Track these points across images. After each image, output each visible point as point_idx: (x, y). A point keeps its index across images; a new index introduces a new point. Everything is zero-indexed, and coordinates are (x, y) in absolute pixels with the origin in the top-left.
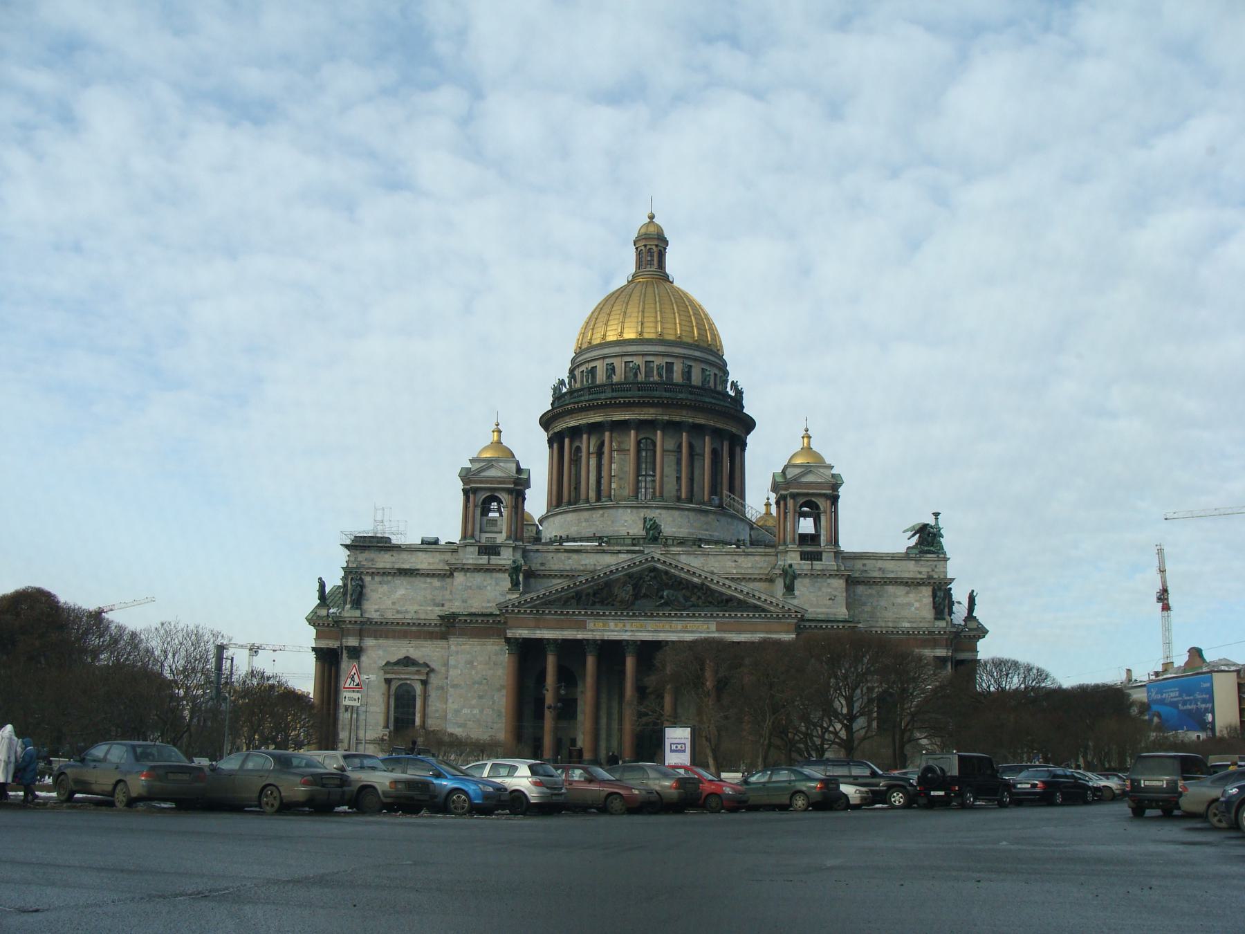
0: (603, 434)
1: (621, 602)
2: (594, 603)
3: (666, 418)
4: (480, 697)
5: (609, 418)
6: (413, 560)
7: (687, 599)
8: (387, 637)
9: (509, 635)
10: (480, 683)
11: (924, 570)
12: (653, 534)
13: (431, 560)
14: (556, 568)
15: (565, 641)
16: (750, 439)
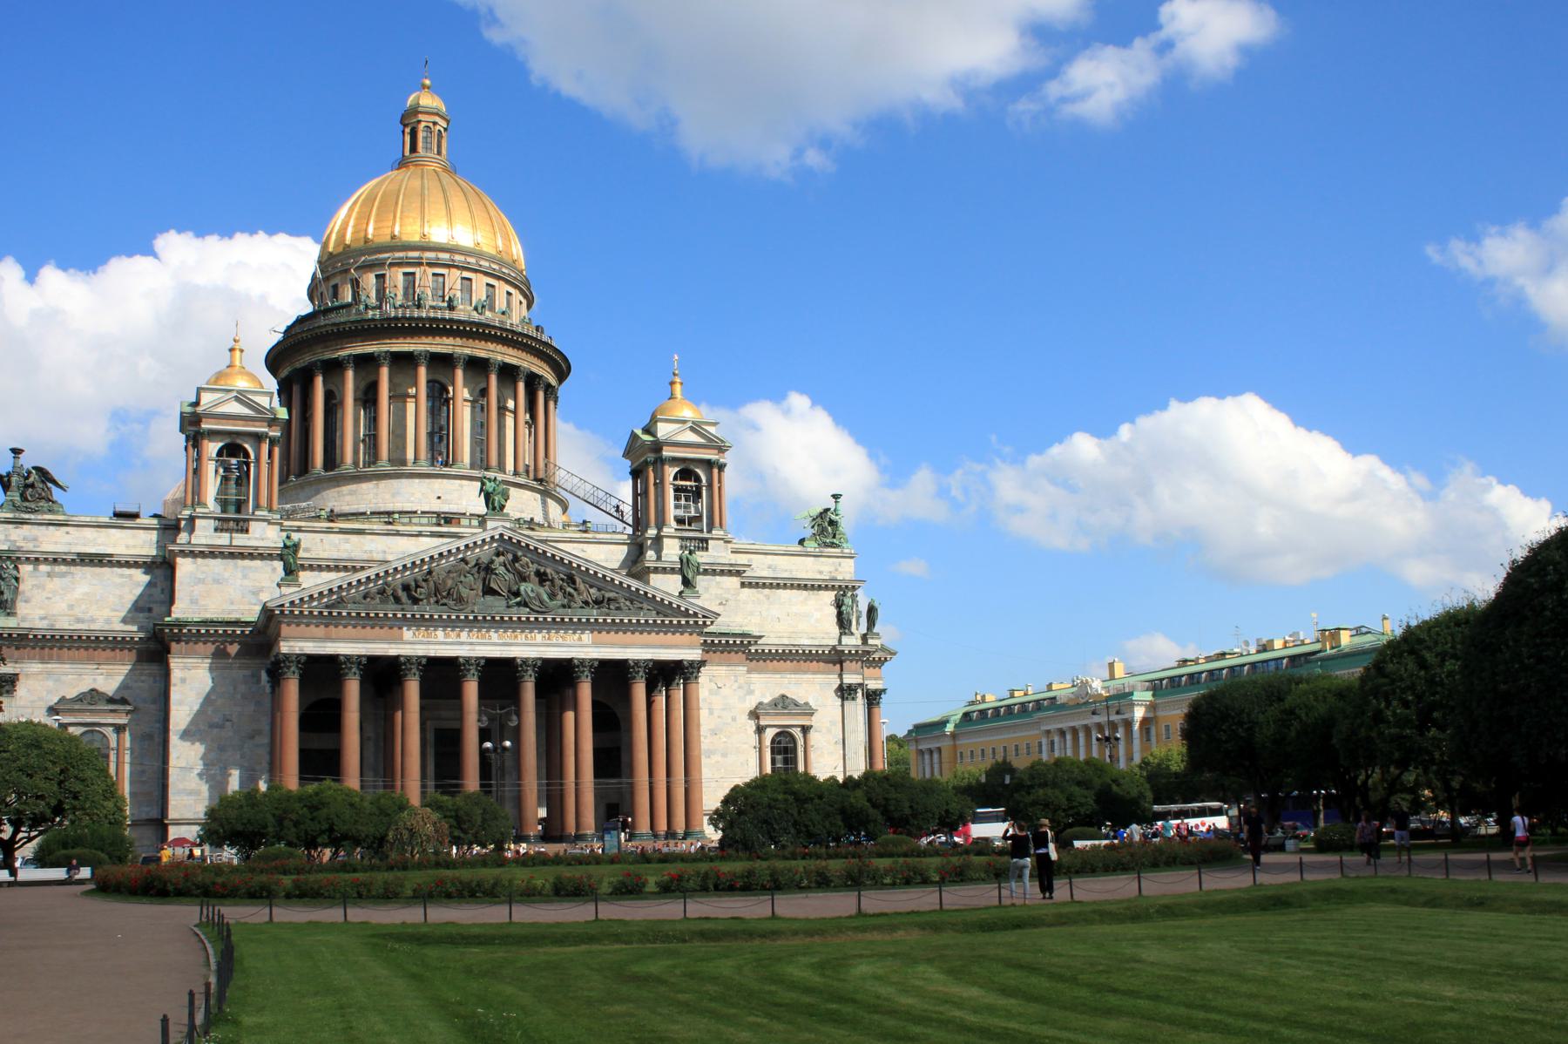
0: (378, 374)
1: (460, 600)
2: (416, 601)
3: (468, 351)
4: (222, 749)
5: (385, 348)
6: (99, 541)
7: (552, 596)
8: (60, 660)
9: (285, 647)
10: (221, 727)
11: (826, 569)
12: (494, 502)
13: (131, 542)
14: (325, 555)
15: (373, 660)
16: (563, 390)
